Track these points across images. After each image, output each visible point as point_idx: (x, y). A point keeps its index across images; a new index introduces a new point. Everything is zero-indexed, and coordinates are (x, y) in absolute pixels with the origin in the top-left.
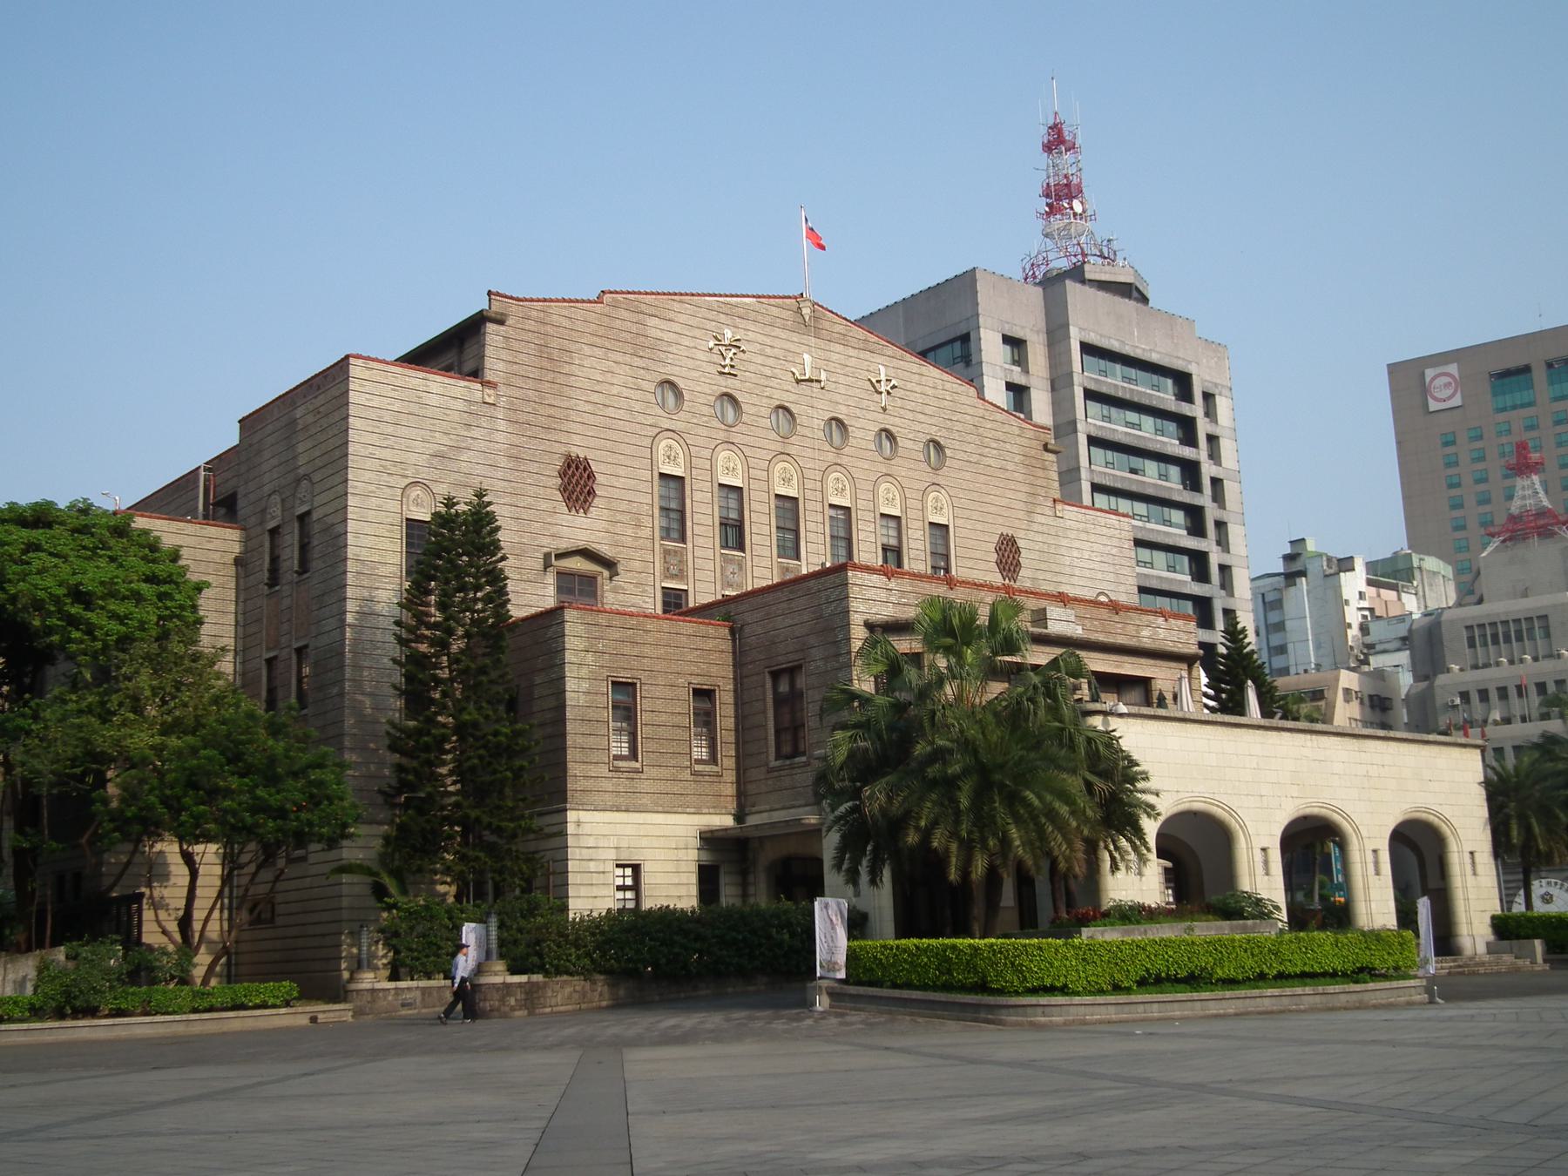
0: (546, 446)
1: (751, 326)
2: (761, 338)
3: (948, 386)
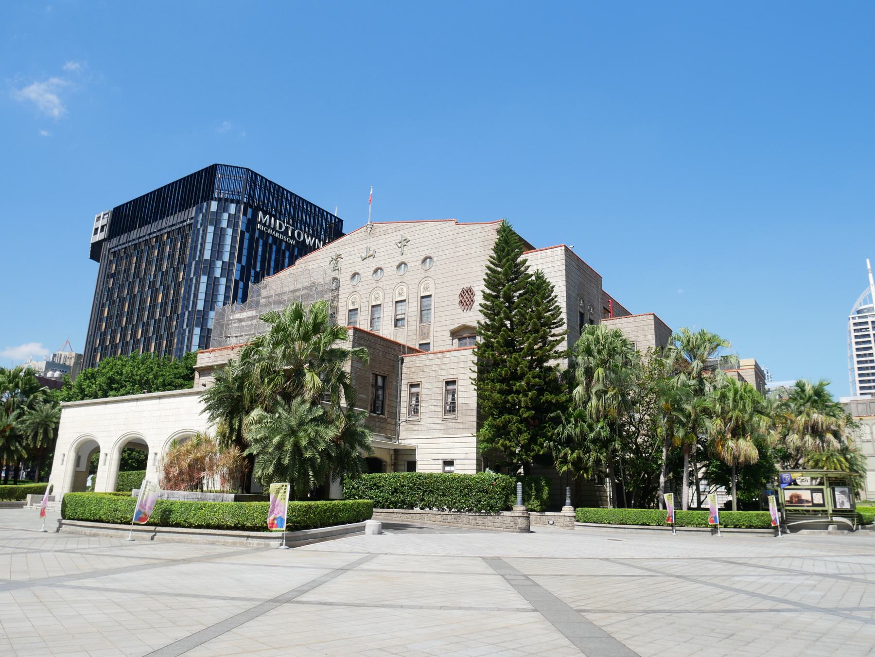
3: (438, 227)
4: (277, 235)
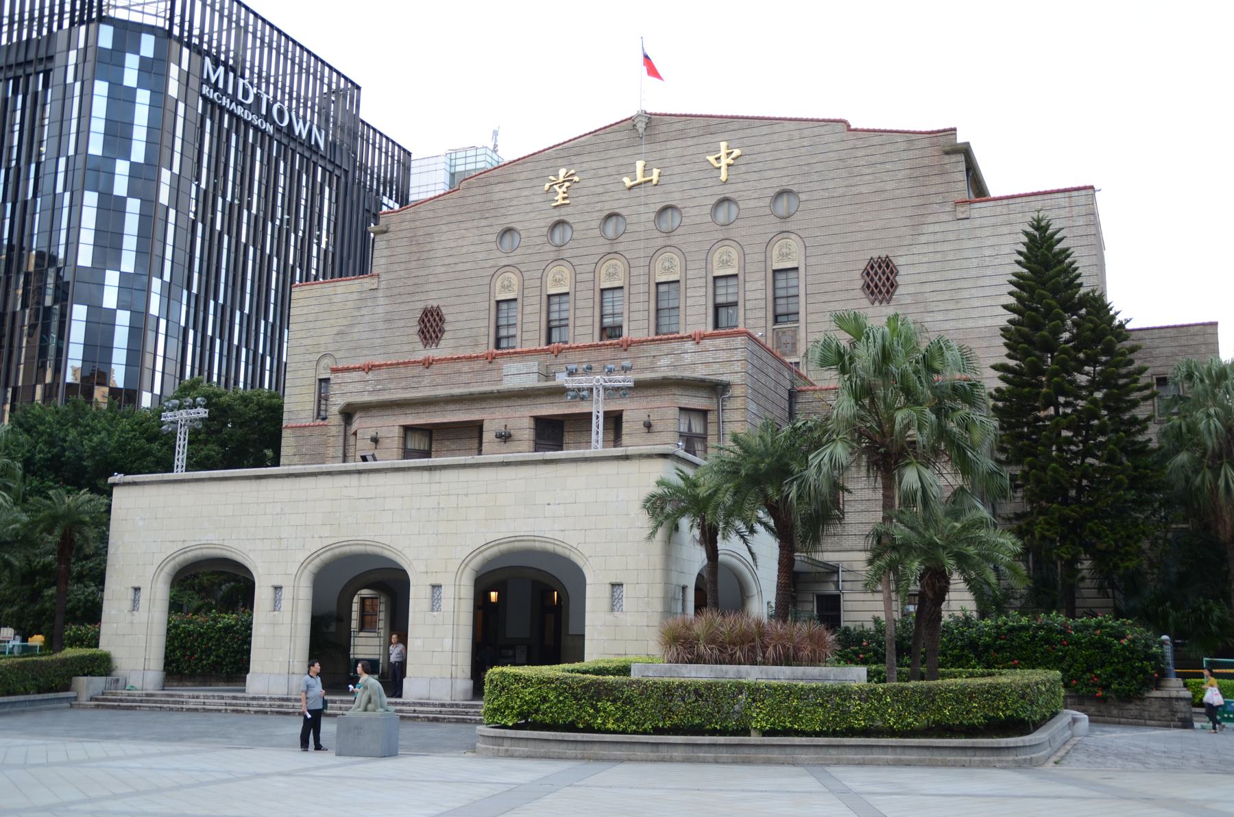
0: (411, 306)
1: (586, 158)
2: (594, 165)
3: (807, 133)
4: (240, 111)
